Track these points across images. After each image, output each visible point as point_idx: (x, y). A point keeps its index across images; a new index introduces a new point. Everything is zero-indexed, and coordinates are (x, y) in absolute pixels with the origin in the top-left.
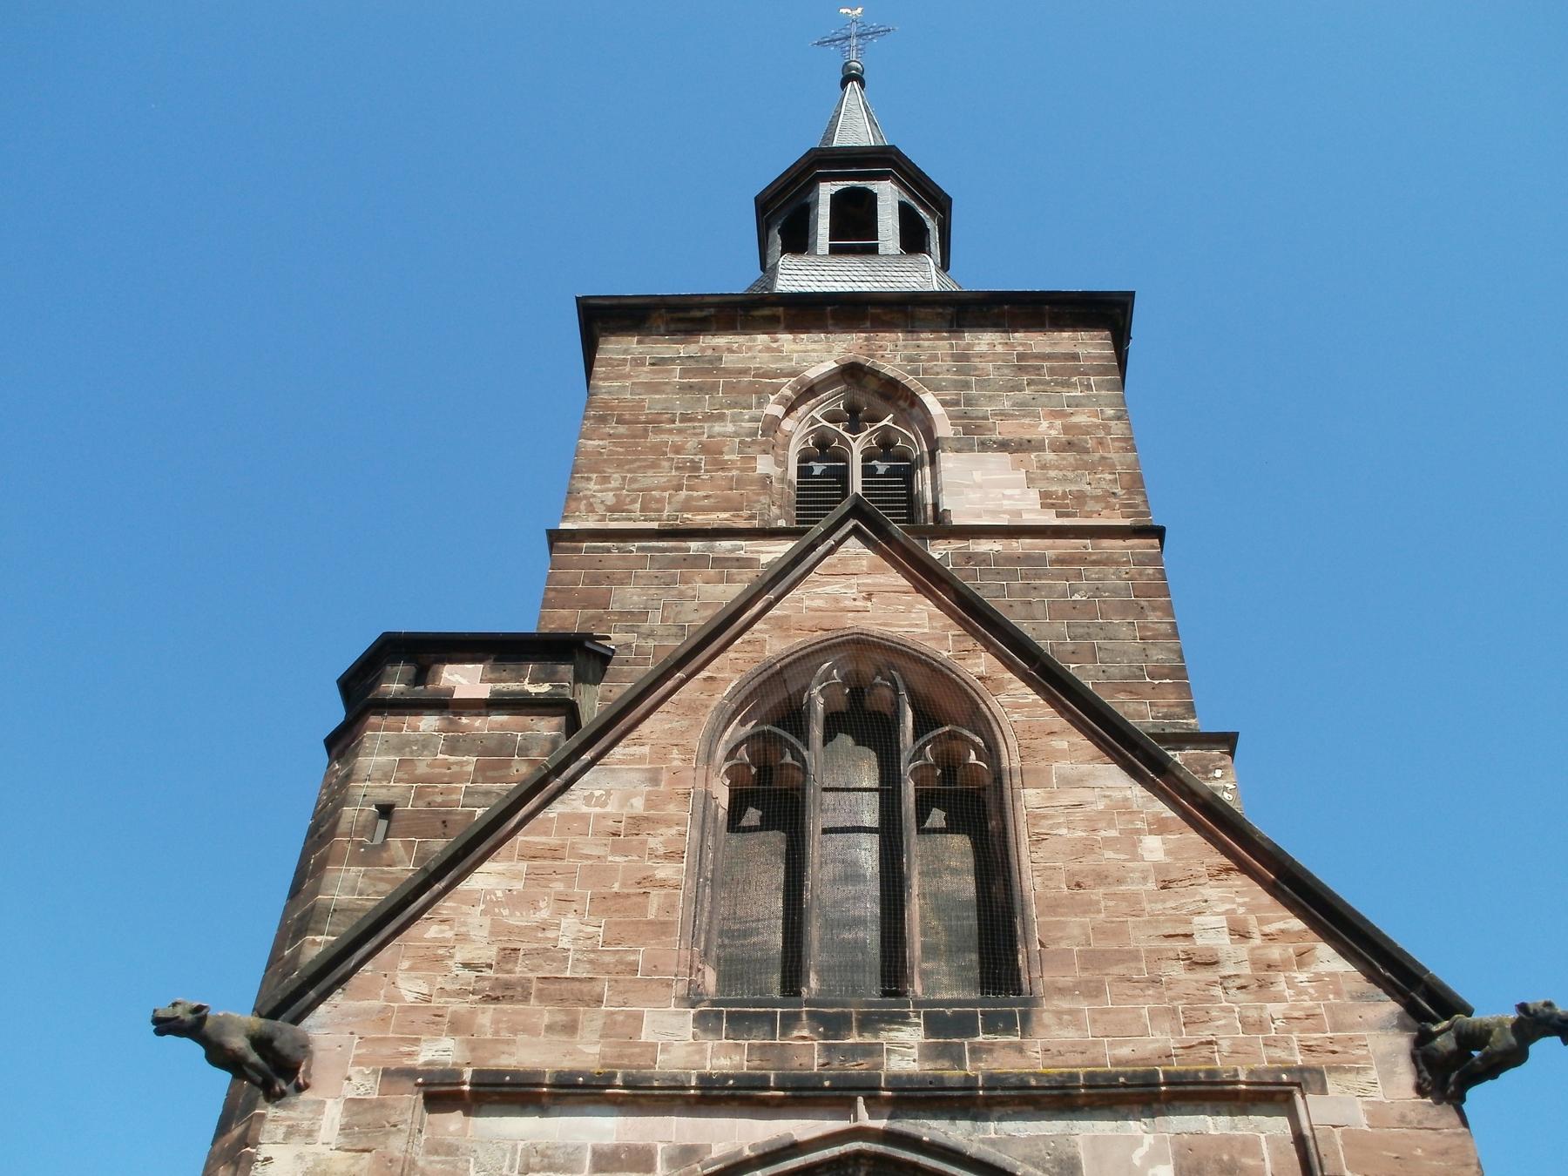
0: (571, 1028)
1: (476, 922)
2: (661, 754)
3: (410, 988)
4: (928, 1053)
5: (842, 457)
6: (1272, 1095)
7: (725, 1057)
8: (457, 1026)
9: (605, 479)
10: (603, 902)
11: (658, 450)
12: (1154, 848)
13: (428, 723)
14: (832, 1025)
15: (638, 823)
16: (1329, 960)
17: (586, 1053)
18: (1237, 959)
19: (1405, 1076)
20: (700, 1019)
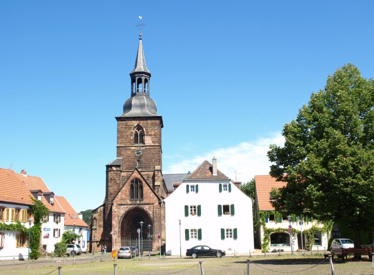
0: (124, 201)
1: (119, 196)
2: (127, 186)
3: (117, 200)
4: (139, 202)
5: (138, 134)
6: (152, 204)
7: (130, 203)
8: (120, 201)
9: (120, 140)
10: (125, 195)
11: (123, 136)
12: (149, 191)
13: (112, 172)
14: (135, 201)
15: (126, 190)
16: (156, 198)
17: (125, 203)
18: (152, 197)
19: (158, 203)
20: (130, 201)
